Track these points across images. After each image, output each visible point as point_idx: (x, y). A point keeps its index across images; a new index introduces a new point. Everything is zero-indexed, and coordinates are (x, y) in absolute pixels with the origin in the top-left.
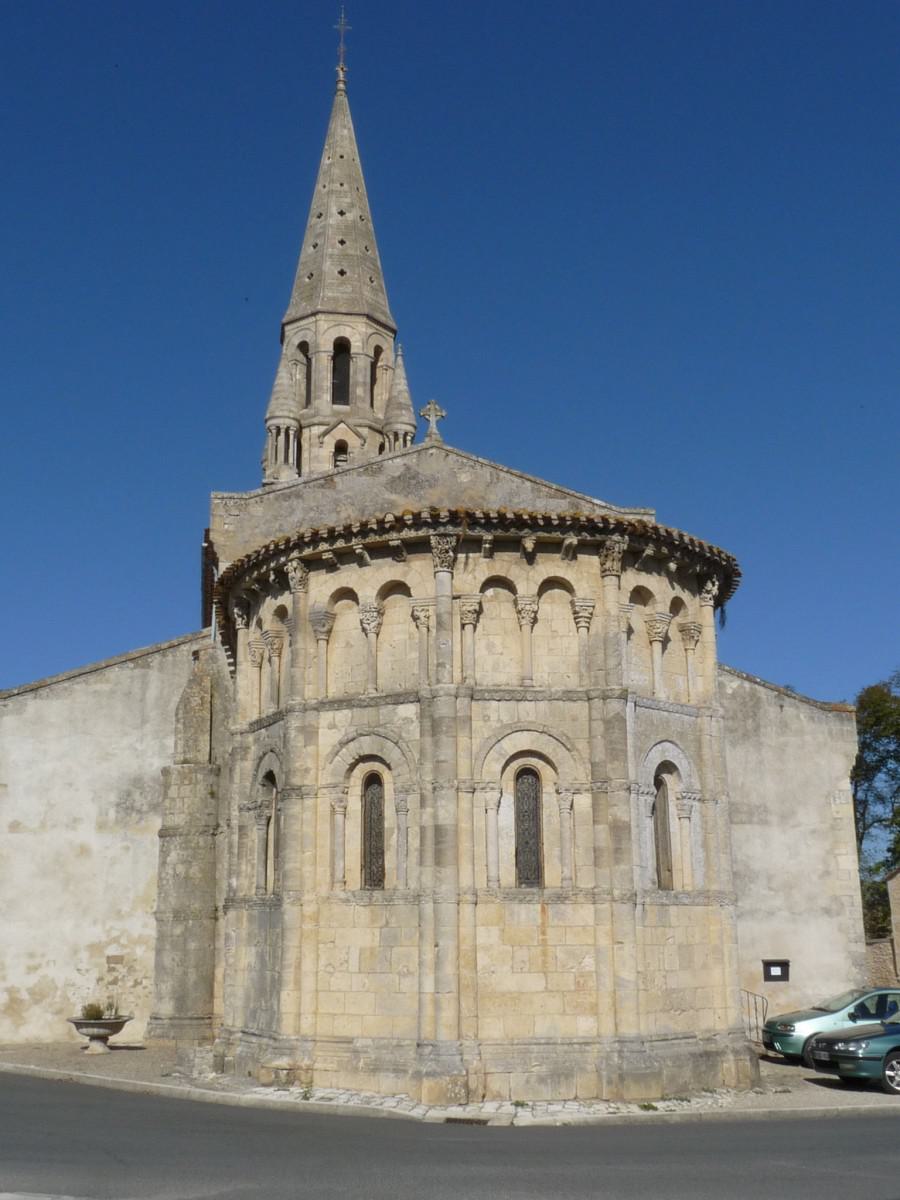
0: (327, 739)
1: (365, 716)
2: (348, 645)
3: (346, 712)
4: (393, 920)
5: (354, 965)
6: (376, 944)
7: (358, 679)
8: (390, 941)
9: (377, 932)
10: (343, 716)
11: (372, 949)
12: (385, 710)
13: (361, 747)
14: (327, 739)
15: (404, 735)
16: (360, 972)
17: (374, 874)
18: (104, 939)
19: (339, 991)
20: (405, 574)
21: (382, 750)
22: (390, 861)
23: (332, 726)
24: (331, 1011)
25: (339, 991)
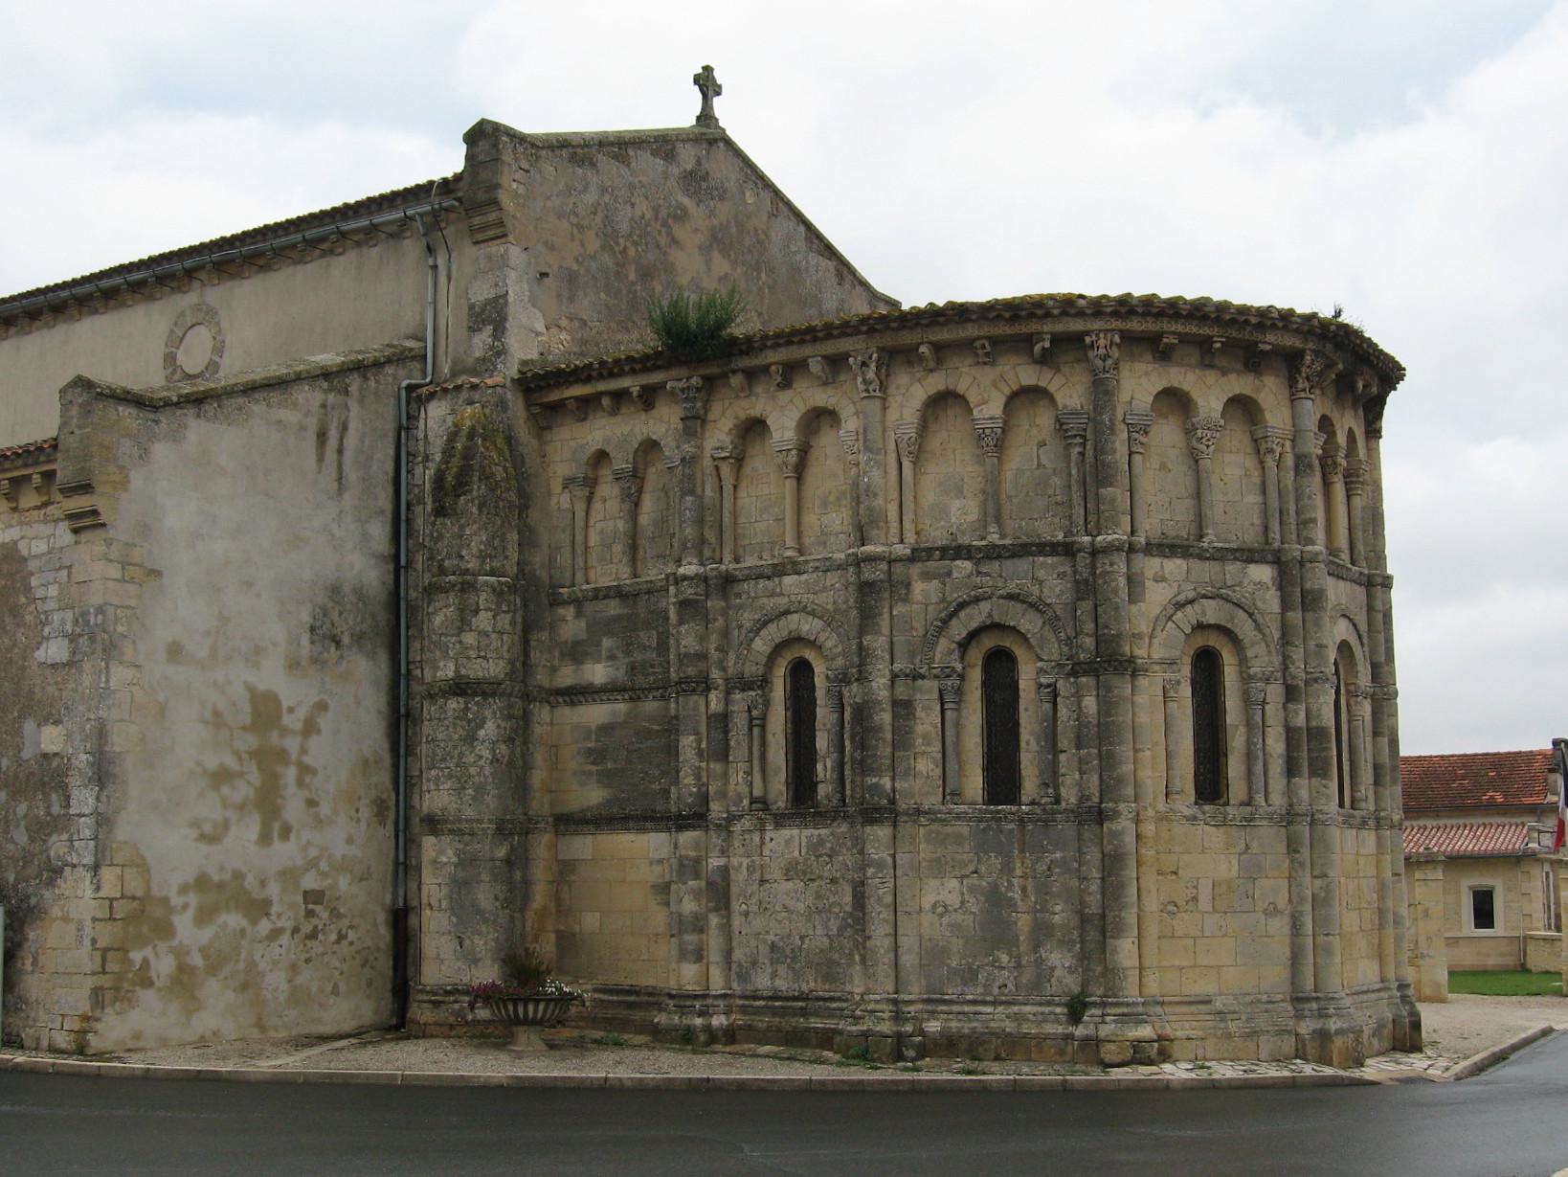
0: (1157, 596)
1: (1207, 571)
2: (1163, 467)
3: (1179, 561)
4: (1254, 845)
5: (1205, 903)
6: (1234, 872)
7: (1178, 518)
8: (1252, 872)
9: (1235, 862)
10: (1175, 566)
11: (1229, 882)
12: (1233, 568)
13: (1204, 613)
14: (1157, 596)
15: (1259, 604)
16: (1215, 910)
17: (1210, 786)
18: (300, 862)
19: (1186, 936)
20: (1258, 390)
21: (1232, 620)
22: (1235, 768)
23: (1160, 579)
24: (1177, 963)
25: (1186, 936)
